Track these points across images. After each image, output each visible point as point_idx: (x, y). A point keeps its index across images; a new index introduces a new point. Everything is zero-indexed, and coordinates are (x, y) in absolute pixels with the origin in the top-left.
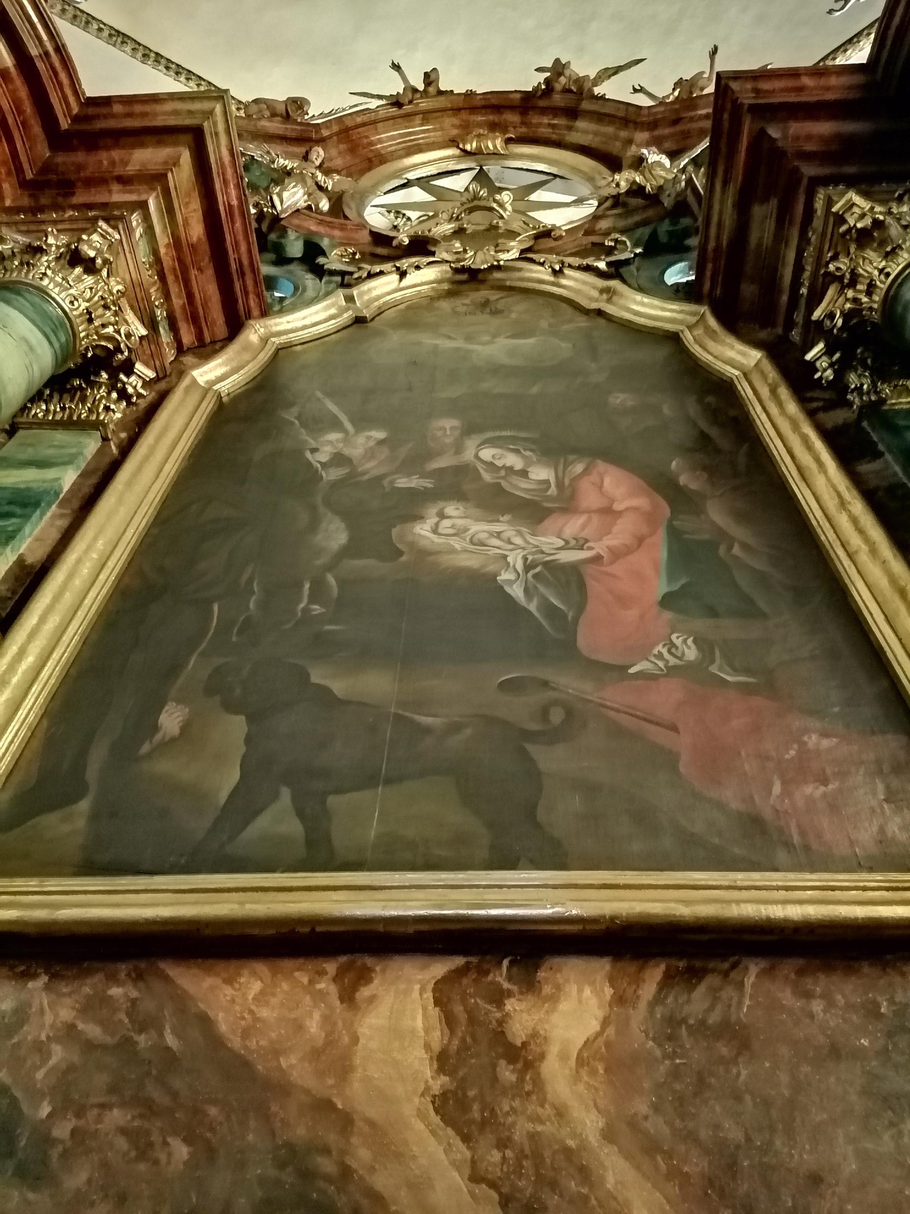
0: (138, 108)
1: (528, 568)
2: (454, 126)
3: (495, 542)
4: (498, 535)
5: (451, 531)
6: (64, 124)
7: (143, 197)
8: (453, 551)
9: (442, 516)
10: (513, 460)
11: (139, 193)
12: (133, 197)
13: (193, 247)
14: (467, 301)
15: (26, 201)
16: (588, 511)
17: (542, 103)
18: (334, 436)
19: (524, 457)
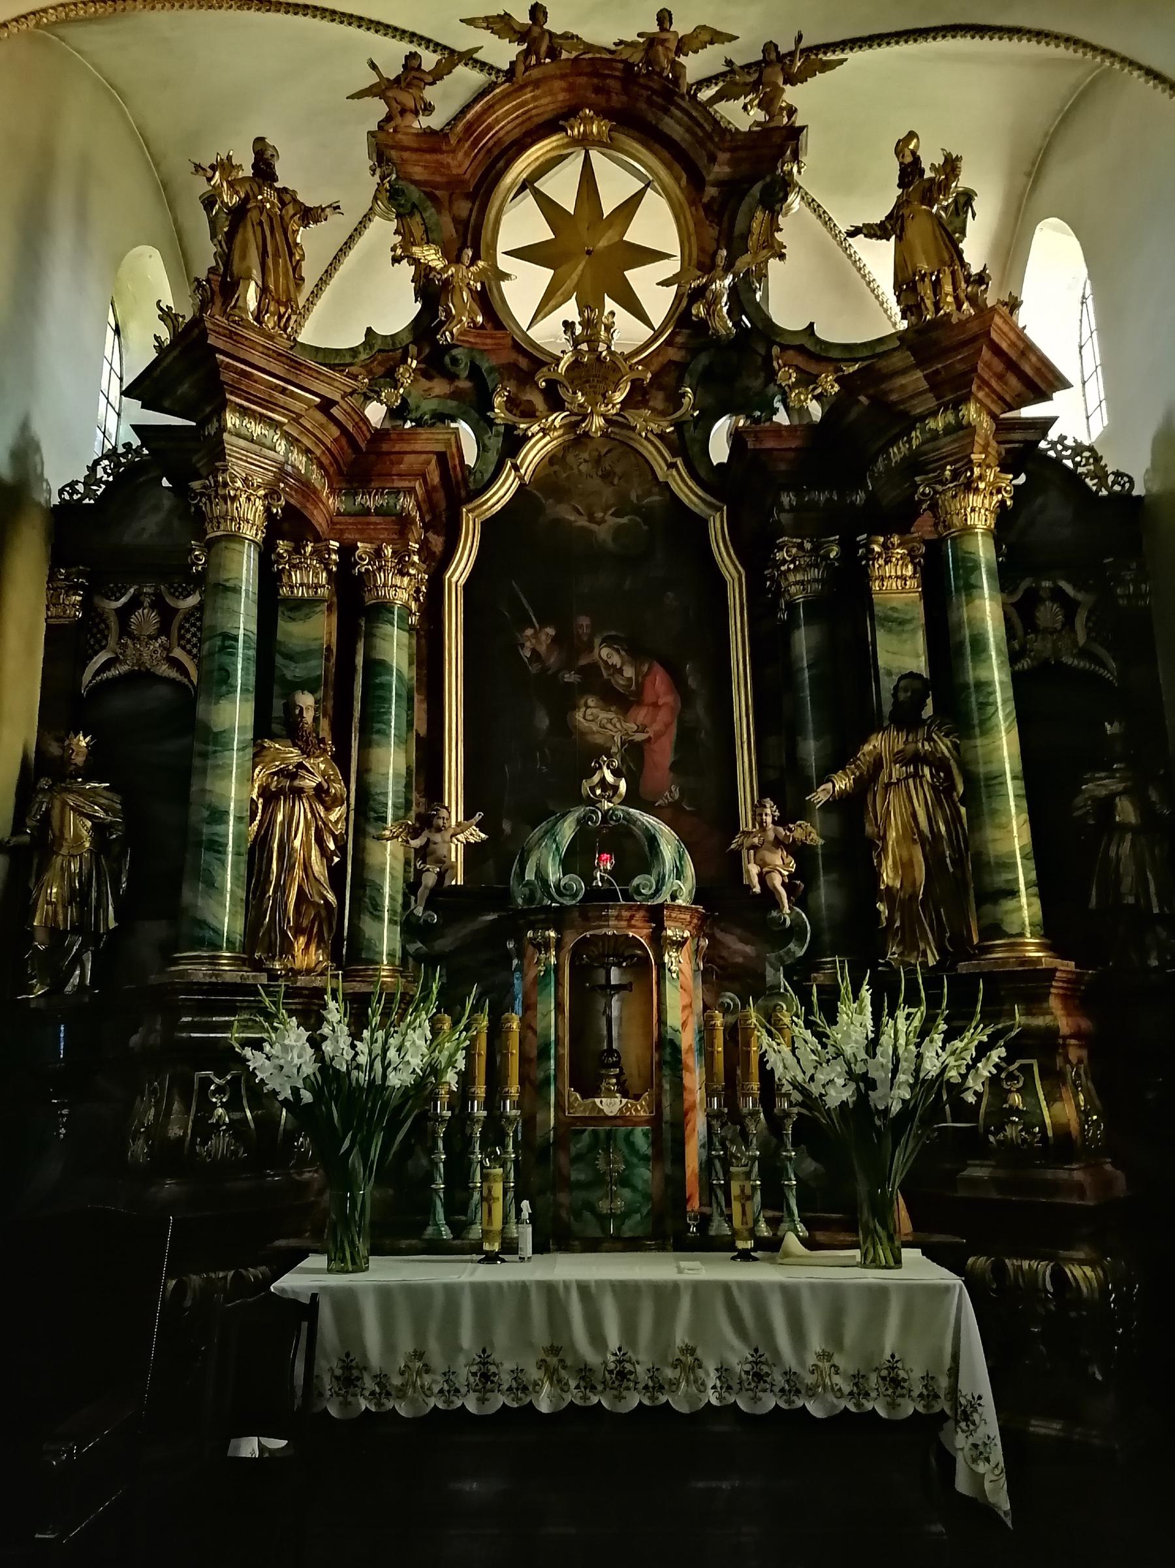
0: (406, 437)
1: (623, 744)
2: (564, 90)
3: (609, 726)
4: (610, 721)
5: (590, 718)
6: (363, 446)
7: (412, 485)
8: (593, 733)
9: (588, 707)
10: (616, 660)
11: (410, 481)
12: (406, 484)
13: (434, 487)
14: (586, 456)
15: (344, 485)
16: (648, 705)
17: (642, 81)
18: (529, 632)
19: (621, 657)
